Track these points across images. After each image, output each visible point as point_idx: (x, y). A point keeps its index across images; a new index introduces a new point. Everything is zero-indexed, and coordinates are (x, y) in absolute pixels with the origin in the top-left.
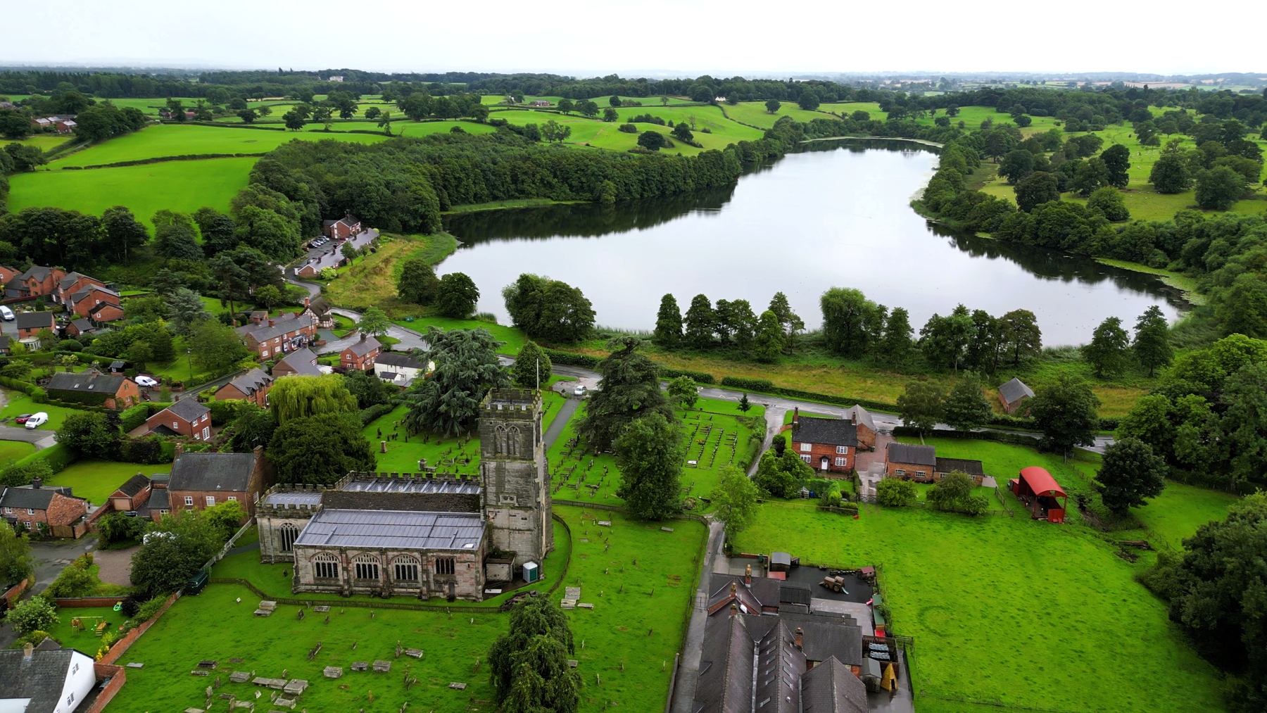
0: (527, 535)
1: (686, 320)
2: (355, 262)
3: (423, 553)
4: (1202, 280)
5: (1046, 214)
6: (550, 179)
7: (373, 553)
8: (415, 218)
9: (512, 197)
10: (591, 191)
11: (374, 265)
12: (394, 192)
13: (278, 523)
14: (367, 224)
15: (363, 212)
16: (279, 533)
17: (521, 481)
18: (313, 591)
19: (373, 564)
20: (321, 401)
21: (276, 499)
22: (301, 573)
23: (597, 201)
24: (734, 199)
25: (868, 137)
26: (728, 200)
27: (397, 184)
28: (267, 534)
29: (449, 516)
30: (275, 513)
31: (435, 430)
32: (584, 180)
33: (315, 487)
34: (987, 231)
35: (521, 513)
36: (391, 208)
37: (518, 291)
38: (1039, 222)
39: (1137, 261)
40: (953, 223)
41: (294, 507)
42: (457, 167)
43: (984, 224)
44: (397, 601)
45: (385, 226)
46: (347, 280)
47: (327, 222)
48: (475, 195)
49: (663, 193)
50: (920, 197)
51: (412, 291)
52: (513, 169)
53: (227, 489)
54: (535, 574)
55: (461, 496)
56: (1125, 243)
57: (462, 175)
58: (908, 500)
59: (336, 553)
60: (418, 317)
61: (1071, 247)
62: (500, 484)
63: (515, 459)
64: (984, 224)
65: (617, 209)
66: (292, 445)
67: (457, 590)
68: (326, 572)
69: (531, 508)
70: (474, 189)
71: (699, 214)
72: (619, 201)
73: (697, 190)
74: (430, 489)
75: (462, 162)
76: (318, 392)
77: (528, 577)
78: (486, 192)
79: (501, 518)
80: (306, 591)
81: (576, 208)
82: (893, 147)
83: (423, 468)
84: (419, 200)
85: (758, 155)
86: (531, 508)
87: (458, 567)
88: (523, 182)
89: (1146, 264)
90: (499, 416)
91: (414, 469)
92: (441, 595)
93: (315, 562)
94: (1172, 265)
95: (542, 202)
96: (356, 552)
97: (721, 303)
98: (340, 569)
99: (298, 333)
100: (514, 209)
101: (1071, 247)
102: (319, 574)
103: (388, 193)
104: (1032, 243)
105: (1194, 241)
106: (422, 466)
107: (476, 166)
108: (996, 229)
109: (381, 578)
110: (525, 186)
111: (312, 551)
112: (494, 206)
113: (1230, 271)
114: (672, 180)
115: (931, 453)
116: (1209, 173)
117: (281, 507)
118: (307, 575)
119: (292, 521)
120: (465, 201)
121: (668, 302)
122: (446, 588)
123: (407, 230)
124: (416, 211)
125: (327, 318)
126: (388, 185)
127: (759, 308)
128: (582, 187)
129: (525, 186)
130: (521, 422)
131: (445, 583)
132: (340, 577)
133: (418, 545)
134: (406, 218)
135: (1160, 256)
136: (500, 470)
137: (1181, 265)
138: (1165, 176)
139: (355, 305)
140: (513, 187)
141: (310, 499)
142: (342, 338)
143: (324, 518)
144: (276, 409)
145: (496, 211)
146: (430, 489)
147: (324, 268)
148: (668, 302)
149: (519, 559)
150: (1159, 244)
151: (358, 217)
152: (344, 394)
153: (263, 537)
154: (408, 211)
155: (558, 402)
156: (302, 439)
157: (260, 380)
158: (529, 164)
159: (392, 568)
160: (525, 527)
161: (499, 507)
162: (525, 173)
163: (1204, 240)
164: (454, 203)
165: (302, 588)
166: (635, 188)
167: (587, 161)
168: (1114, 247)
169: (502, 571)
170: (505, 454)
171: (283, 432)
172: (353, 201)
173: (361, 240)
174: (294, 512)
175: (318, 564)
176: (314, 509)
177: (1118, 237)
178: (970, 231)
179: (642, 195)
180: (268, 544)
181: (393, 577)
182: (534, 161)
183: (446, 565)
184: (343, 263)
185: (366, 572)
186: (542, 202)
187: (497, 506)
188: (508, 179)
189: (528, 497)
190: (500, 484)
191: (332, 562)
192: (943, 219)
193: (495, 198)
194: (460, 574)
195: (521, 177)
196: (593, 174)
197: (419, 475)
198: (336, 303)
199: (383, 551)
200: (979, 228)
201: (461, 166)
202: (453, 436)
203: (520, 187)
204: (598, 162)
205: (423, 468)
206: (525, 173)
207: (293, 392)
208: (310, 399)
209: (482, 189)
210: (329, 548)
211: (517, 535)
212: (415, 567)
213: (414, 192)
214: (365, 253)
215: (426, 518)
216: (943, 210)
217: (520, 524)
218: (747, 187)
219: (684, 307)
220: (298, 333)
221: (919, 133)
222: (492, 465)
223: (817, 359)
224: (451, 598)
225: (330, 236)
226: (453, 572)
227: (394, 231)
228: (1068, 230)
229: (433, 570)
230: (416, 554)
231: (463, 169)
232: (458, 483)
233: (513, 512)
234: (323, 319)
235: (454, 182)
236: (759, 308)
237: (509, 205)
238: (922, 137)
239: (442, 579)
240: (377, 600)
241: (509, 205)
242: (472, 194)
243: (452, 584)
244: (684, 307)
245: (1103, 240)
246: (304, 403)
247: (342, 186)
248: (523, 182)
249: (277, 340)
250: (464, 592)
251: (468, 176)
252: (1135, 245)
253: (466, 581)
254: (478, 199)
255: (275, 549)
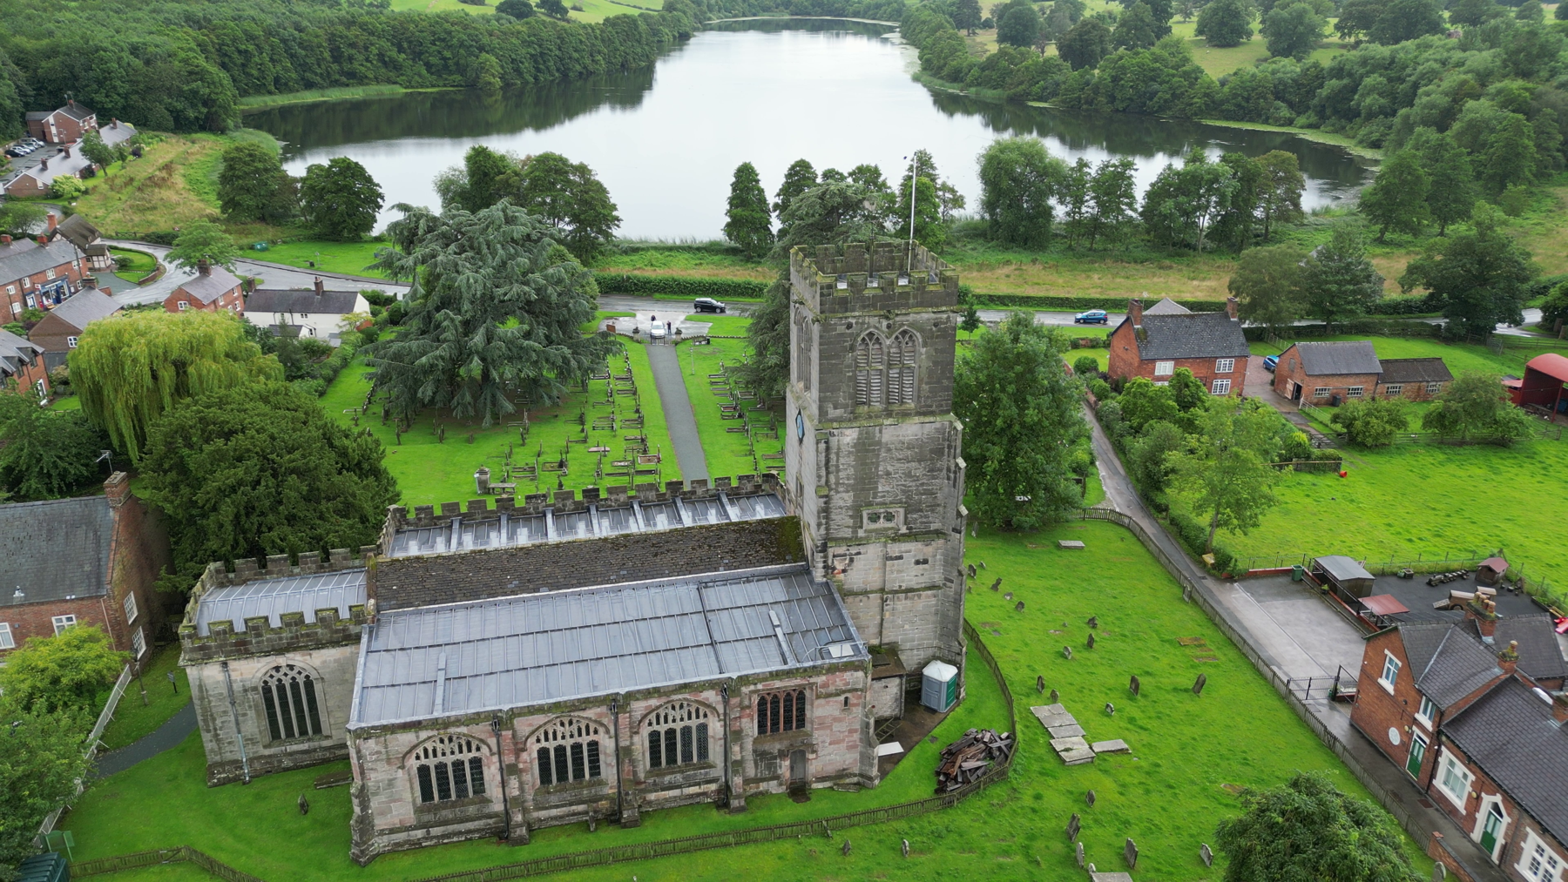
0: (927, 601)
1: (776, 206)
2: (113, 169)
3: (727, 689)
4: (1363, 132)
5: (1123, 67)
6: (394, 53)
7: (591, 713)
8: (193, 106)
9: (336, 84)
10: (461, 70)
11: (145, 175)
12: (148, 62)
13: (251, 670)
14: (105, 118)
15: (97, 98)
16: (259, 697)
17: (919, 470)
18: (416, 846)
19: (585, 740)
20: (208, 367)
21: (219, 606)
22: (375, 804)
23: (474, 88)
24: (656, 86)
25: (787, 17)
26: (650, 87)
27: (152, 49)
28: (218, 706)
29: (726, 581)
30: (239, 642)
31: (458, 413)
32: (447, 54)
33: (326, 557)
34: (1040, 99)
35: (913, 549)
36: (149, 89)
37: (466, 181)
38: (1115, 79)
39: (1251, 120)
40: (989, 94)
41: (298, 619)
42: (239, 34)
43: (1035, 89)
44: (666, 831)
45: (143, 122)
46: (106, 198)
47: (33, 115)
48: (277, 80)
49: (565, 76)
50: (917, 68)
51: (248, 200)
52: (332, 38)
53: (46, 594)
54: (956, 683)
55: (740, 527)
56: (1235, 96)
57: (251, 48)
58: (1399, 435)
59: (482, 730)
60: (274, 243)
61: (1161, 109)
62: (864, 484)
63: (905, 415)
64: (1035, 89)
65: (505, 98)
66: (218, 458)
67: (816, 766)
68: (444, 786)
69: (939, 533)
70: (273, 70)
71: (613, 108)
72: (507, 86)
73: (609, 73)
74: (511, 536)
75: (246, 25)
76: (199, 347)
77: (940, 701)
78: (294, 75)
79: (864, 570)
80: (396, 849)
81: (439, 101)
82: (816, 28)
83: (485, 489)
84: (196, 74)
85: (667, 34)
86: (939, 533)
87: (818, 710)
88: (351, 59)
89: (1266, 122)
90: (869, 304)
91: (463, 492)
92: (773, 787)
93: (413, 763)
94: (1302, 120)
95: (387, 90)
96: (539, 719)
97: (829, 174)
98: (491, 773)
99: (51, 275)
100: (343, 102)
101: (1161, 109)
102: (427, 794)
103: (137, 63)
104: (1107, 109)
105: (1333, 84)
106: (483, 485)
107: (269, 33)
108: (1054, 94)
109: (609, 772)
110: (356, 65)
111: (408, 738)
112: (310, 97)
113: (1432, 106)
114: (576, 55)
115: (1367, 354)
116: (1285, 14)
117: (257, 626)
118: (393, 800)
119: (297, 659)
120: (260, 89)
121: (746, 179)
122: (784, 767)
123: (182, 125)
124: (195, 93)
125: (100, 251)
126: (135, 50)
127: (894, 178)
128: (446, 67)
129: (356, 65)
130: (926, 316)
131: (782, 755)
132: (493, 789)
133: (702, 669)
134: (179, 106)
135: (1285, 112)
136: (866, 449)
137: (1314, 119)
138: (1222, 24)
139: (141, 232)
140: (335, 67)
141: (339, 593)
142: (141, 284)
143: (391, 635)
144: (96, 397)
145: (315, 106)
146: (511, 536)
147: (59, 176)
148: (746, 179)
149: (909, 660)
150: (1279, 95)
151: (89, 106)
152: (250, 353)
153: (209, 717)
154: (181, 94)
155: (634, 351)
156: (239, 441)
157: (13, 352)
158: (355, 31)
159: (641, 744)
160: (923, 581)
161: (860, 542)
162: (352, 45)
163: (1345, 81)
164: (244, 93)
165: (380, 843)
166: (527, 66)
167: (447, 26)
168: (1222, 102)
169: (887, 697)
170: (878, 406)
171: (183, 431)
172: (76, 78)
173: (113, 136)
174: (298, 634)
175: (423, 771)
176: (358, 615)
177: (1226, 89)
178: (1017, 101)
179: (536, 78)
180: (228, 731)
181: (644, 763)
182: (364, 26)
183: (783, 712)
184: (87, 173)
185: (563, 766)
186: (387, 90)
187: (855, 541)
188: (327, 55)
189: (933, 507)
190: (864, 484)
191: (466, 757)
192: (973, 89)
193: (309, 85)
194: (823, 725)
195: (347, 51)
196: (462, 44)
197: (477, 506)
198: (102, 230)
199: (617, 704)
200: (1027, 95)
201: (245, 32)
202: (500, 421)
203: (347, 66)
204: (466, 27)
205: (485, 489)
206: (352, 45)
207: (139, 348)
208: (180, 366)
209: (285, 69)
210: (458, 722)
211: (901, 604)
212: (703, 728)
213: (186, 61)
214: (122, 158)
215: (670, 595)
216: (969, 79)
217: (909, 575)
218: (667, 71)
219: (771, 185)
220: (51, 275)
221: (851, 9)
222: (849, 436)
223: (976, 252)
224: (799, 791)
225: (44, 136)
226: (801, 722)
227: (160, 127)
228: (1156, 86)
229: (750, 727)
230: (711, 696)
231: (251, 37)
232: (582, 510)
233: (895, 549)
234: (91, 253)
235: (239, 60)
236: (894, 178)
237: (335, 95)
238: (856, 15)
239: (776, 747)
240: (610, 838)
241: (335, 95)
242: (270, 79)
243: (799, 755)
244: (771, 185)
245: (1206, 95)
246: (167, 375)
247: (52, 53)
248: (351, 59)
249: (12, 290)
250: (831, 770)
251: (259, 48)
252: (1247, 100)
253: (834, 742)
254: (281, 86)
255: (251, 741)
